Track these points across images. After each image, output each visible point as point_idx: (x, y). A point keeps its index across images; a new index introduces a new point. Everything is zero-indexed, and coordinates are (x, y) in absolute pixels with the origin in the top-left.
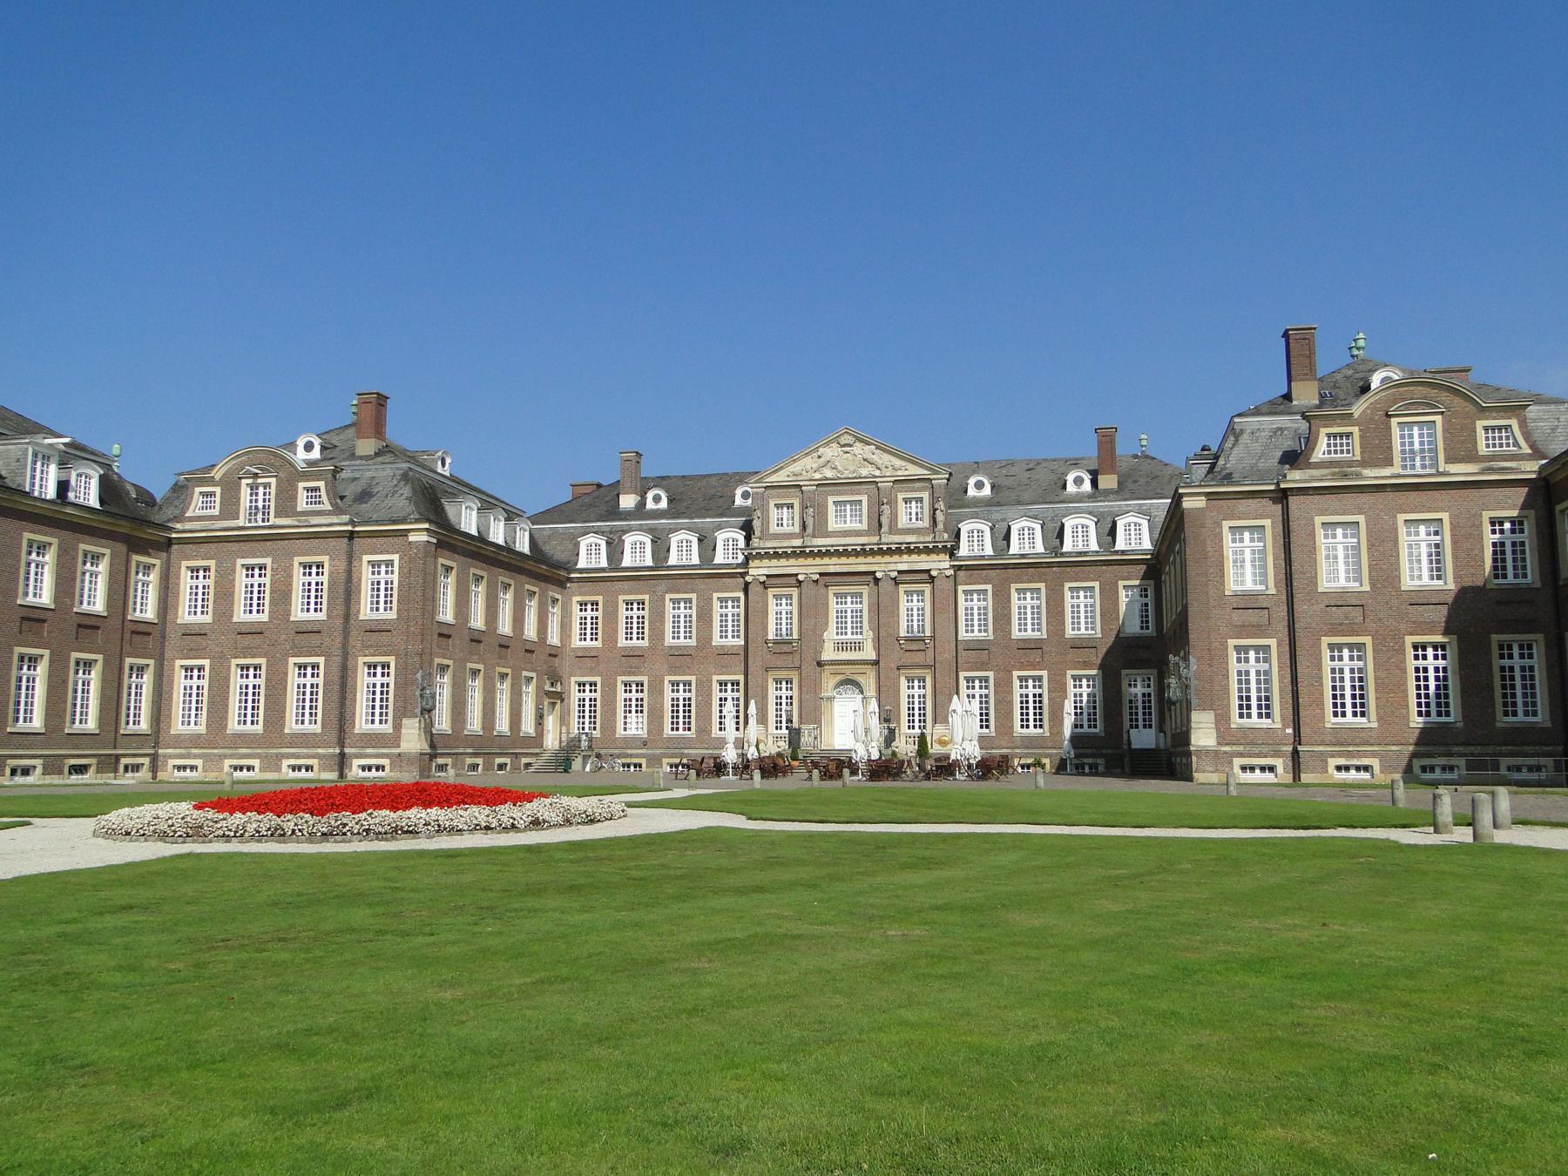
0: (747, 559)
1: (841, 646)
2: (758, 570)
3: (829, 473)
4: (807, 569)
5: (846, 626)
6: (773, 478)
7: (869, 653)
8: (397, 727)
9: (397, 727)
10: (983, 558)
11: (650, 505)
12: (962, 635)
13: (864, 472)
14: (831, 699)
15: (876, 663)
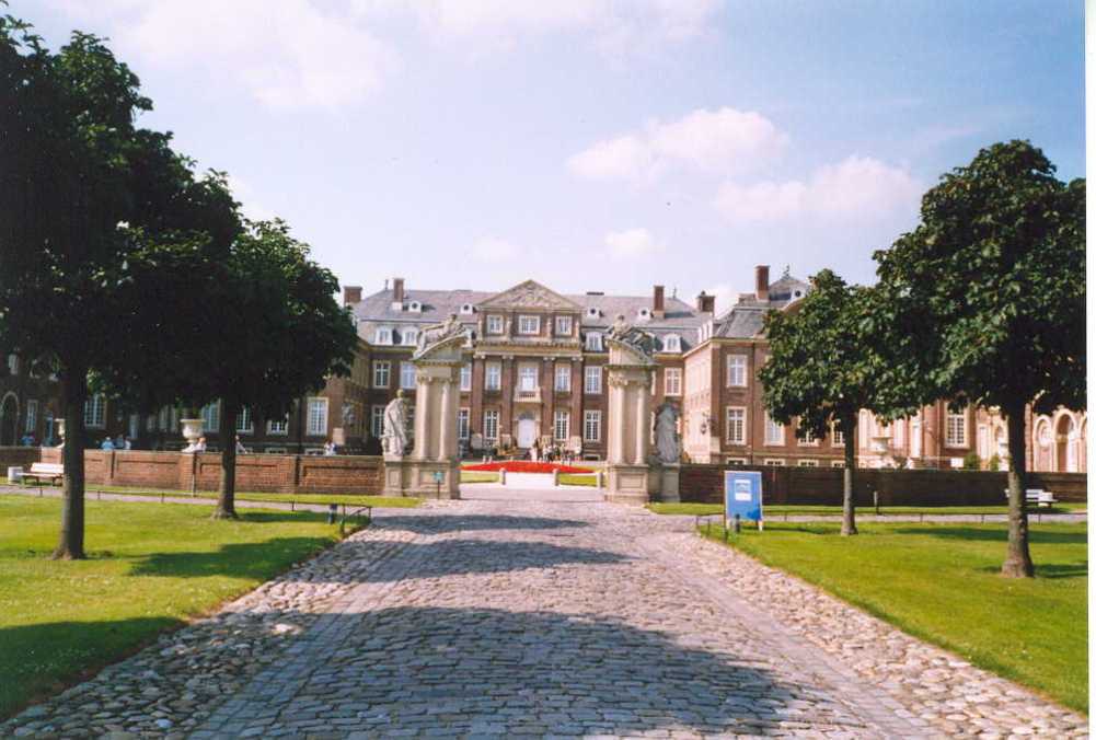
0: (474, 346)
1: (524, 394)
2: (480, 353)
3: (521, 304)
4: (509, 354)
5: (528, 382)
6: (491, 304)
7: (537, 399)
8: (330, 431)
9: (330, 431)
10: (598, 352)
11: (411, 309)
12: (586, 391)
13: (539, 304)
14: (517, 422)
15: (542, 406)
